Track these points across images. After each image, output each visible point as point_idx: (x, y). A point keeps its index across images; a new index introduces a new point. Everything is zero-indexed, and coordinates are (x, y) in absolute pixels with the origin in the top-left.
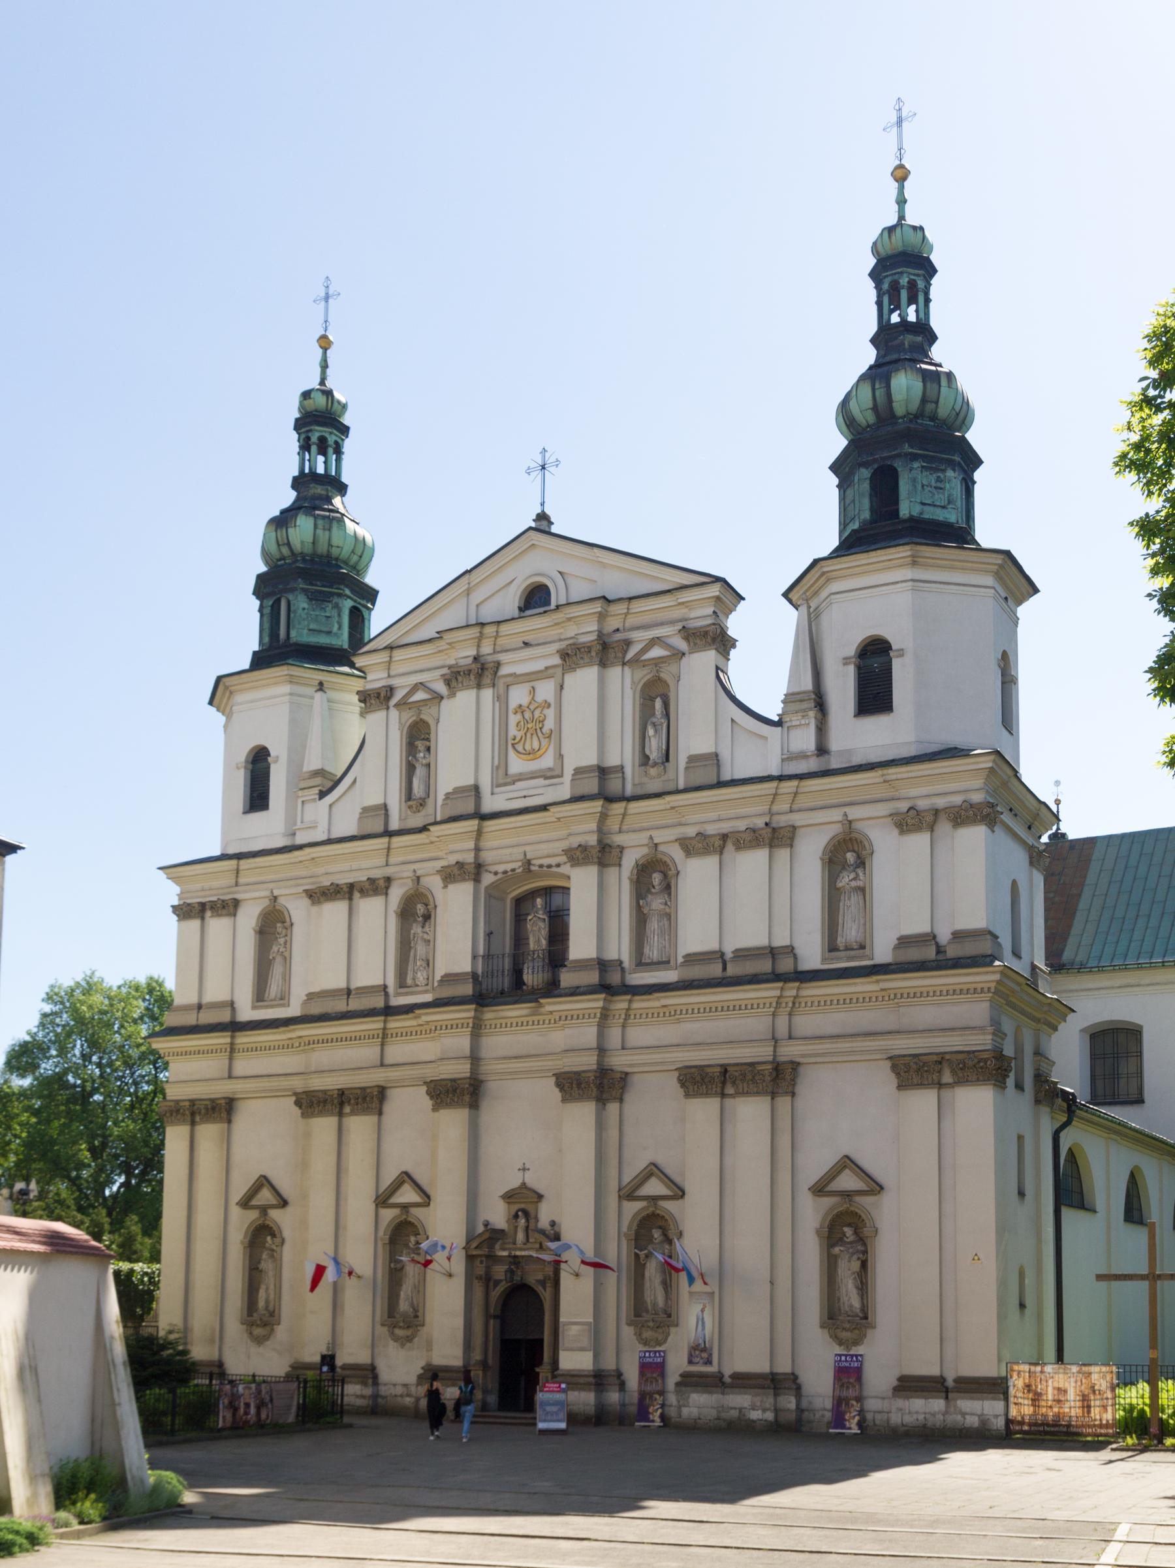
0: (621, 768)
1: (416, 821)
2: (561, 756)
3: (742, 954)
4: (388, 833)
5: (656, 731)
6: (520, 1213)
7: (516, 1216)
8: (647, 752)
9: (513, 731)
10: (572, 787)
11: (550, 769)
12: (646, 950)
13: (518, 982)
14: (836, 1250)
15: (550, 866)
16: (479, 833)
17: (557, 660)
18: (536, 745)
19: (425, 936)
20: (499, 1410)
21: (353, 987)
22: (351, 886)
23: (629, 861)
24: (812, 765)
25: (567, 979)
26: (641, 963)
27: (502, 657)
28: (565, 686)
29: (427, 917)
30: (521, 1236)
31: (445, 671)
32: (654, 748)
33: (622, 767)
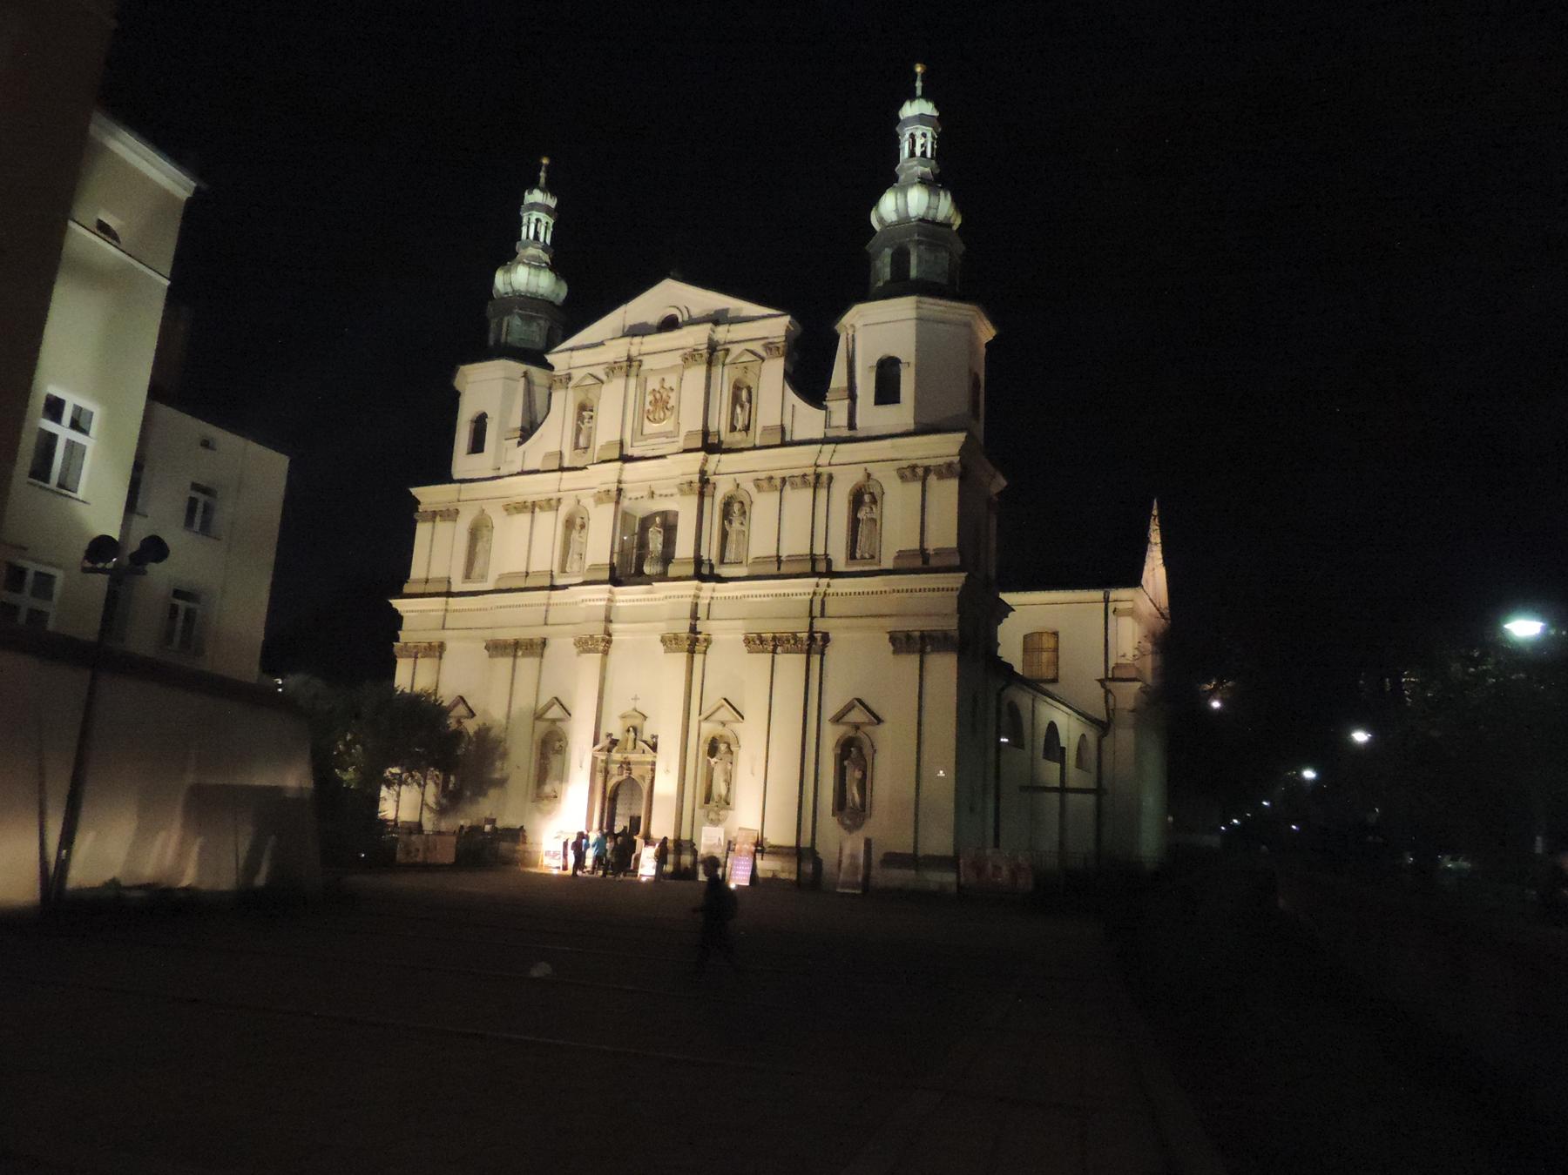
3: (793, 559)
4: (562, 469)
6: (631, 729)
7: (628, 731)
8: (735, 424)
9: (648, 407)
10: (685, 445)
11: (671, 432)
12: (727, 554)
13: (640, 572)
14: (846, 763)
16: (621, 470)
17: (679, 361)
18: (662, 414)
19: (580, 539)
21: (531, 570)
22: (534, 504)
24: (845, 433)
25: (673, 571)
26: (722, 561)
27: (644, 358)
28: (684, 378)
29: (583, 526)
30: (630, 745)
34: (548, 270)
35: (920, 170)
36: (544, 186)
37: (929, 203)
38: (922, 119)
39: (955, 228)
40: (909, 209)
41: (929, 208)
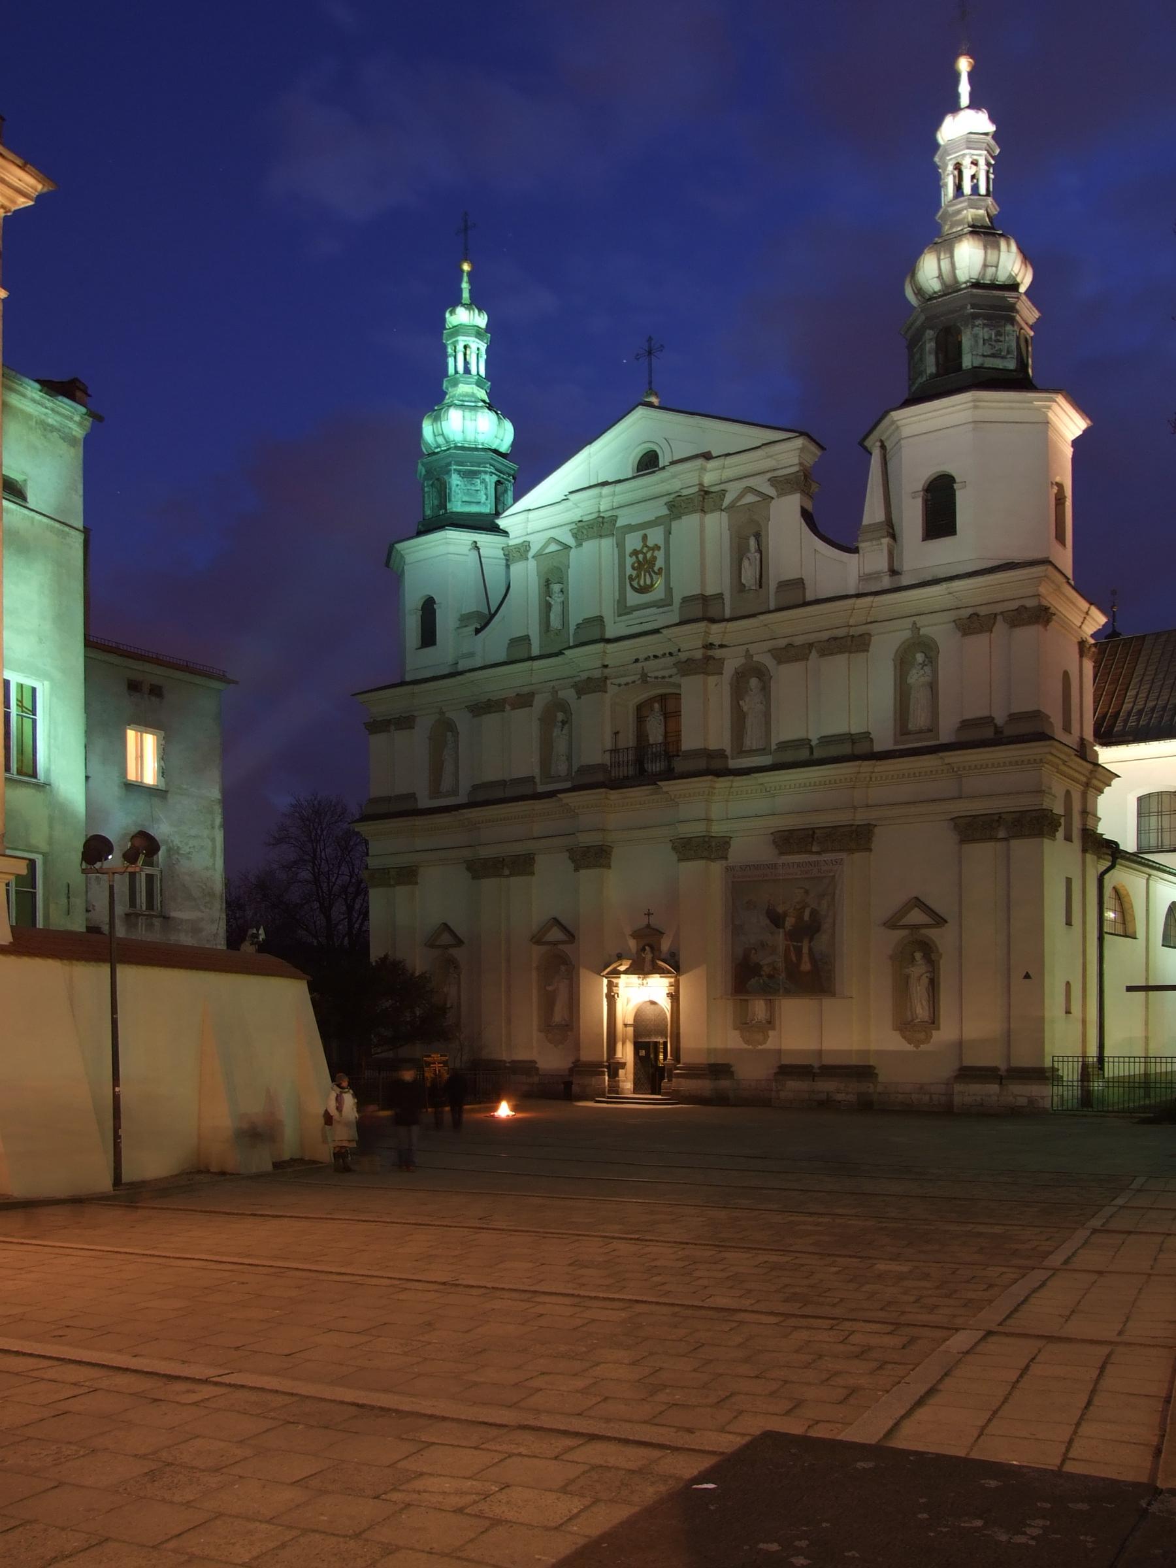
0: (720, 596)
2: (669, 590)
5: (750, 564)
8: (744, 581)
13: (642, 771)
15: (663, 677)
17: (664, 511)
18: (648, 582)
23: (730, 667)
26: (741, 752)
31: (573, 526)
32: (749, 575)
33: (722, 594)
34: (486, 410)
35: (970, 214)
36: (468, 301)
37: (985, 259)
38: (970, 141)
39: (1022, 289)
40: (957, 272)
41: (985, 266)
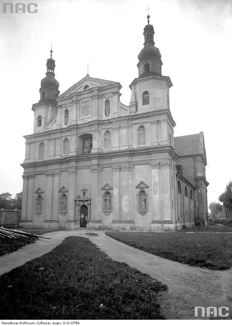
1: (66, 126)
20: (80, 227)
